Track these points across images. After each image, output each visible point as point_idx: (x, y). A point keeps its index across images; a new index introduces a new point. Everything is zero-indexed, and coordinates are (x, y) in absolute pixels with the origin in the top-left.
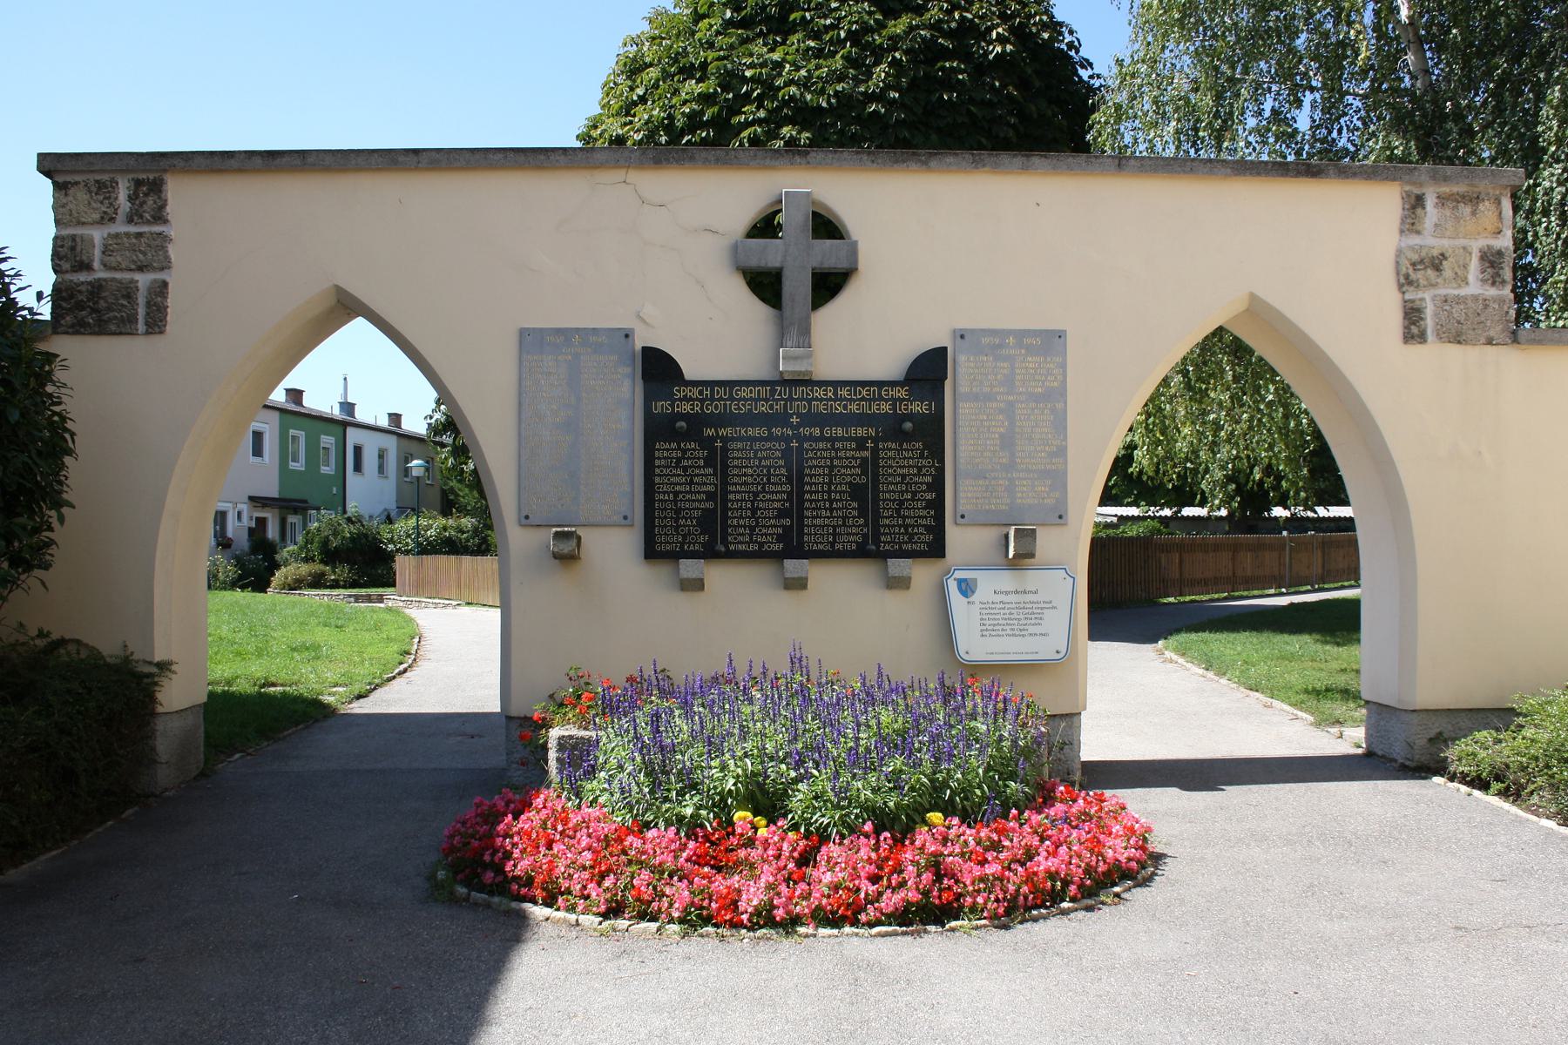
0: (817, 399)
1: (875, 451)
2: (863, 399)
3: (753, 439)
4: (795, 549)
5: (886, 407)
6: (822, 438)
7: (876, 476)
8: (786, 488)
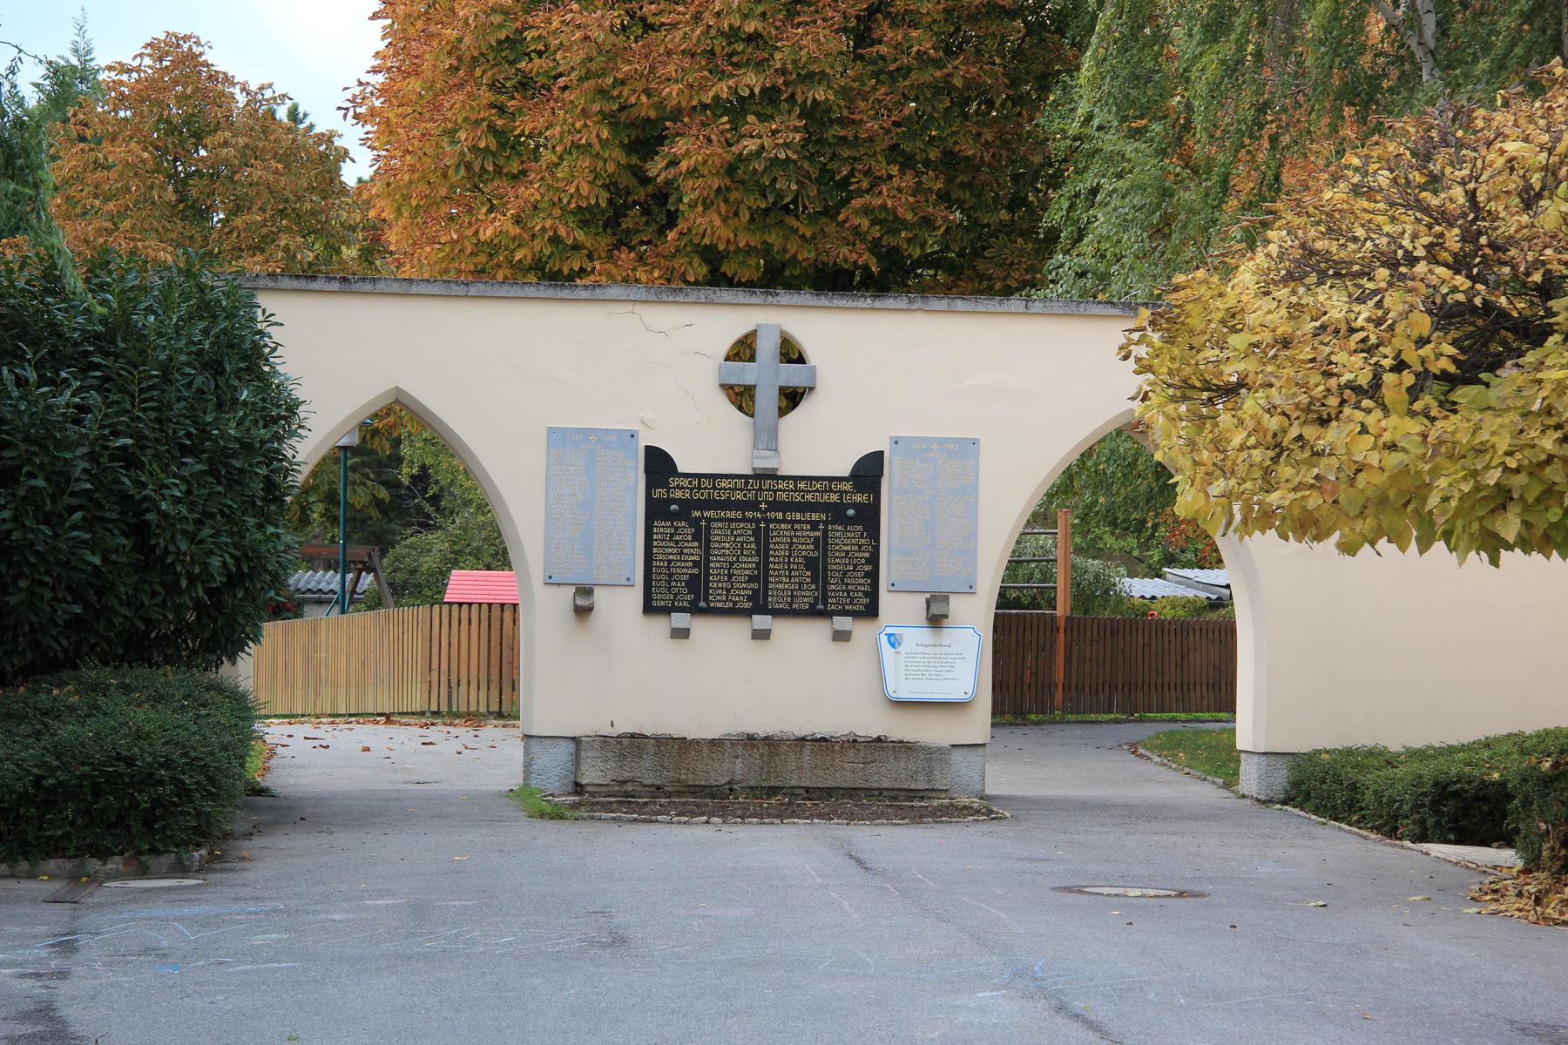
1: (825, 531)
3: (730, 520)
4: (759, 605)
5: (834, 498)
6: (784, 521)
7: (825, 550)
8: (755, 559)
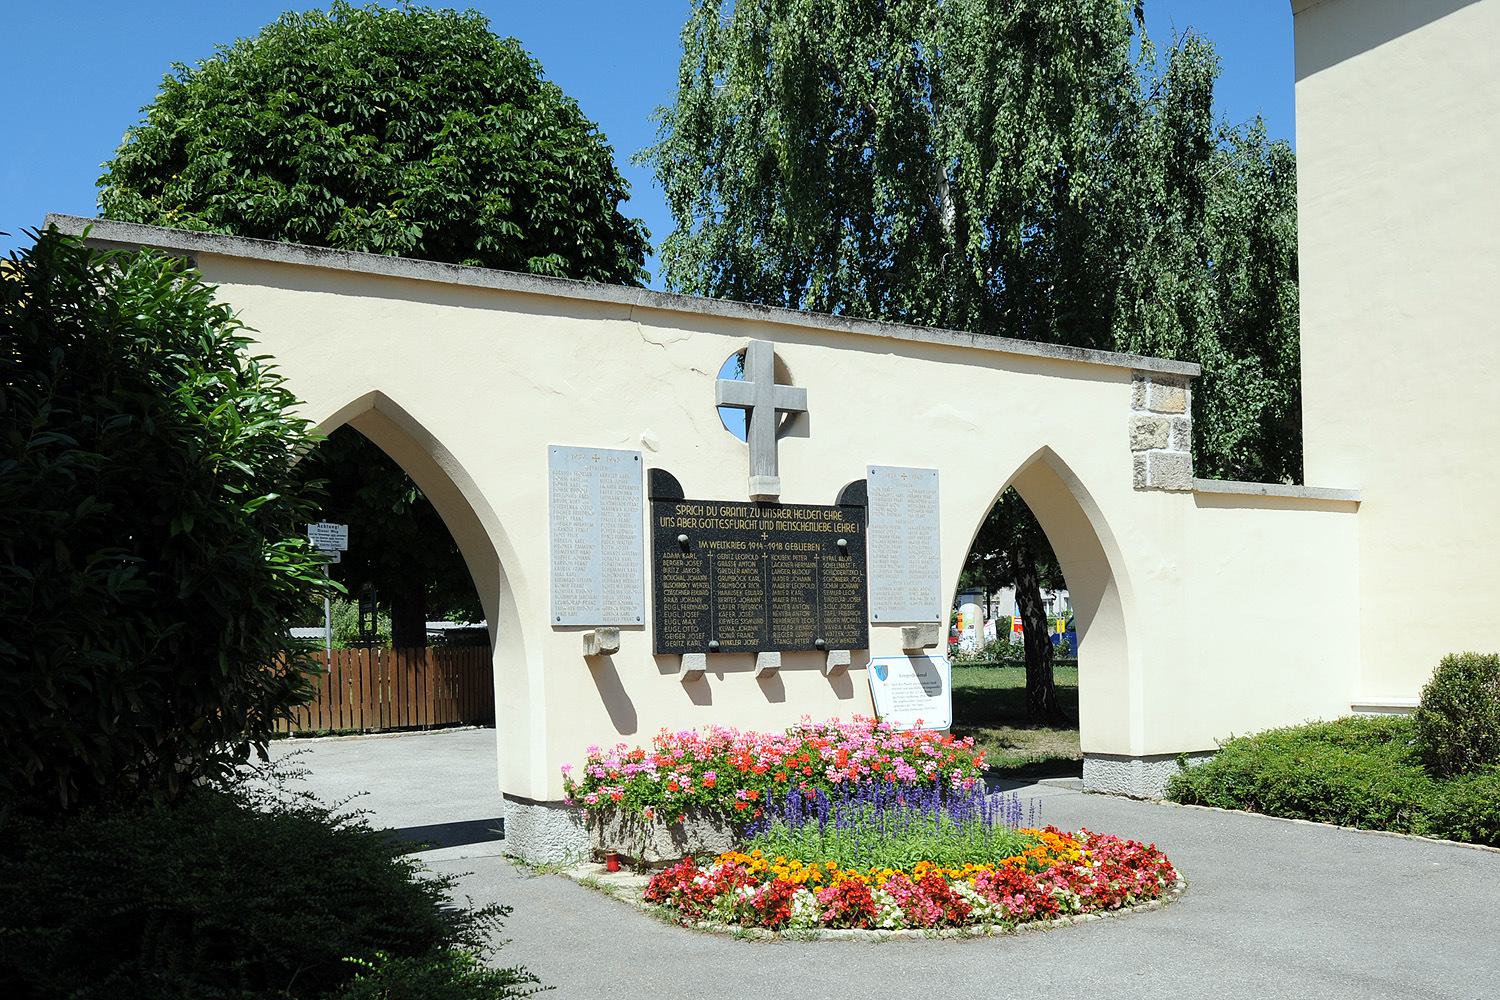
0: (779, 519)
1: (820, 562)
2: (811, 520)
5: (827, 527)
6: (783, 552)
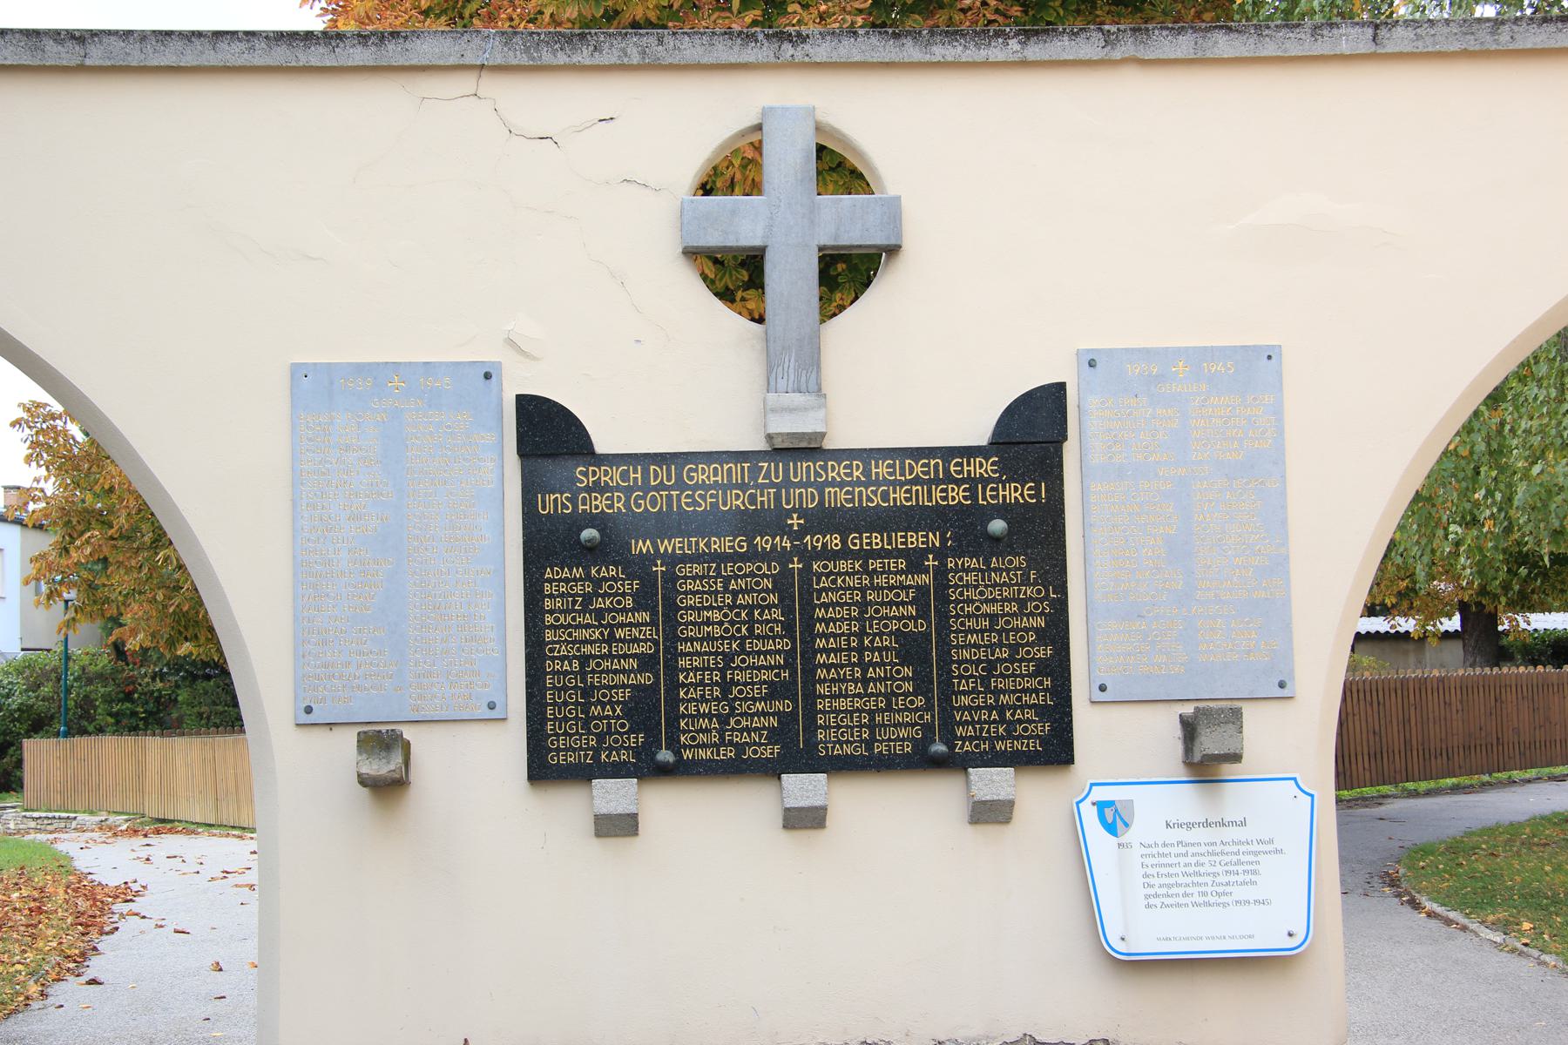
0: (833, 483)
1: (941, 573)
5: (958, 495)
6: (844, 553)
